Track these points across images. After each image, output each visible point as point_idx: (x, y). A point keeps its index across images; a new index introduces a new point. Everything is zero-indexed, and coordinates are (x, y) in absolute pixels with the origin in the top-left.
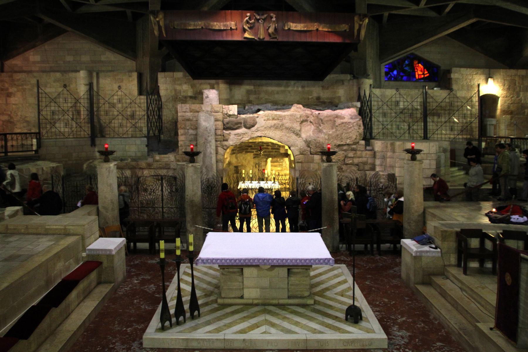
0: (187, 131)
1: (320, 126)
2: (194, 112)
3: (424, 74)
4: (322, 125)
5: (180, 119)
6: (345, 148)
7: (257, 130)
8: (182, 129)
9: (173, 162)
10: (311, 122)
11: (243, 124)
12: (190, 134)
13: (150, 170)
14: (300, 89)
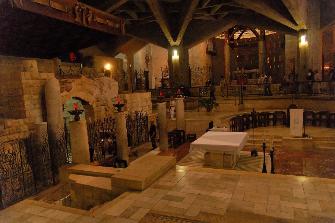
0: (31, 96)
1: (102, 87)
2: (35, 79)
3: (74, 58)
4: (103, 87)
5: (24, 86)
6: (114, 100)
7: (73, 93)
8: (27, 94)
9: (22, 125)
10: (95, 85)
11: (65, 88)
12: (33, 99)
13: (3, 137)
14: (10, 65)
